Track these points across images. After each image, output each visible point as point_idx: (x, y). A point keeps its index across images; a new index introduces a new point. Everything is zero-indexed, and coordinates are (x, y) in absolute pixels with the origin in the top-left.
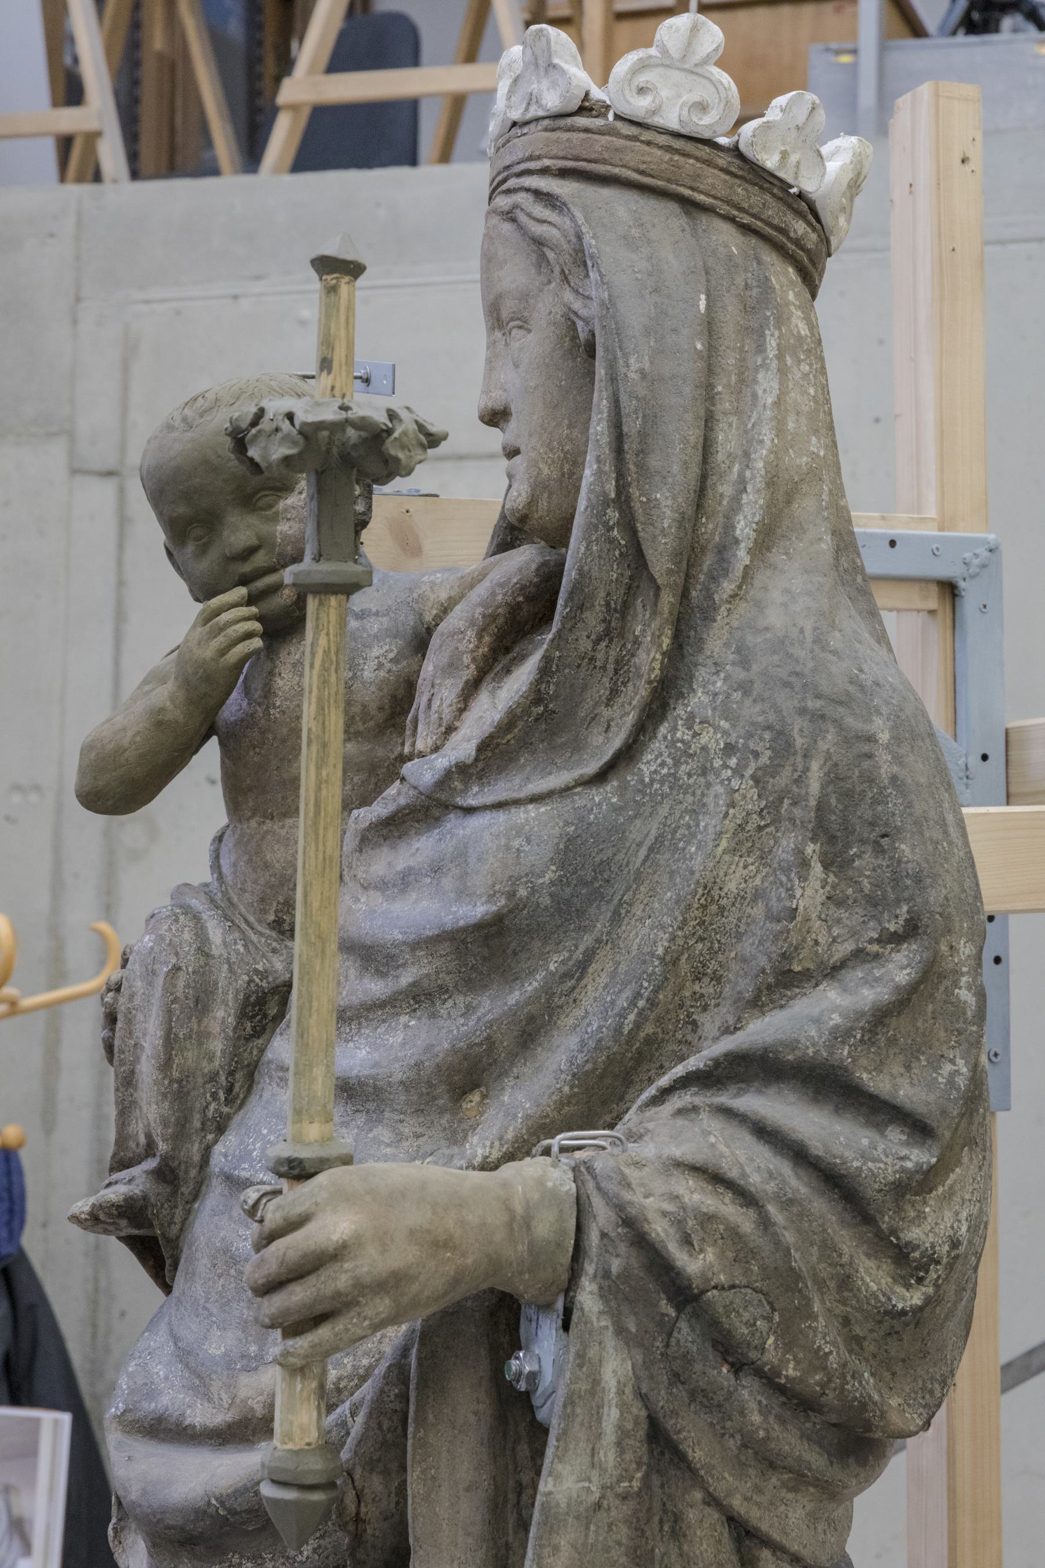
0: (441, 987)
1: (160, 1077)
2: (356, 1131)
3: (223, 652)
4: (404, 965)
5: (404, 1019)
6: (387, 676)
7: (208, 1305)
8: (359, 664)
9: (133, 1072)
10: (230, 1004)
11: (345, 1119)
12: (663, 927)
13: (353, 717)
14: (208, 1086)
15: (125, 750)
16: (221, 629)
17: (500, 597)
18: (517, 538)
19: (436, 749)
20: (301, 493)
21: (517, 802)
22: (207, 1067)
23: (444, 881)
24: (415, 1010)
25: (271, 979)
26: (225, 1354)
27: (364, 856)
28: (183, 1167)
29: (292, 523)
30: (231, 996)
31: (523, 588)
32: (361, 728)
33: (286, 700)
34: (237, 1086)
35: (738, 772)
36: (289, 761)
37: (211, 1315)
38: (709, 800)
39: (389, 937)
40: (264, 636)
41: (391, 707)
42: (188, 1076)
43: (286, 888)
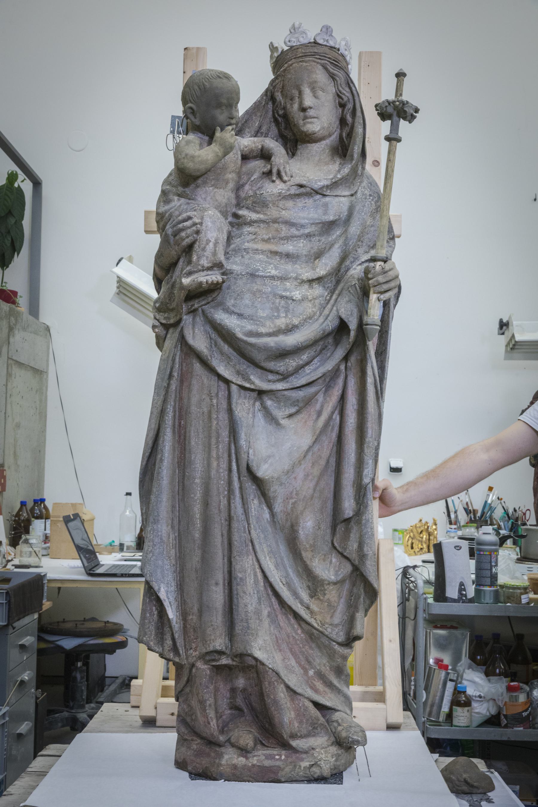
5: (302, 241)
9: (205, 247)
12: (358, 229)
19: (289, 180)
21: (340, 196)
26: (267, 316)
27: (281, 202)
35: (372, 200)
38: (366, 205)
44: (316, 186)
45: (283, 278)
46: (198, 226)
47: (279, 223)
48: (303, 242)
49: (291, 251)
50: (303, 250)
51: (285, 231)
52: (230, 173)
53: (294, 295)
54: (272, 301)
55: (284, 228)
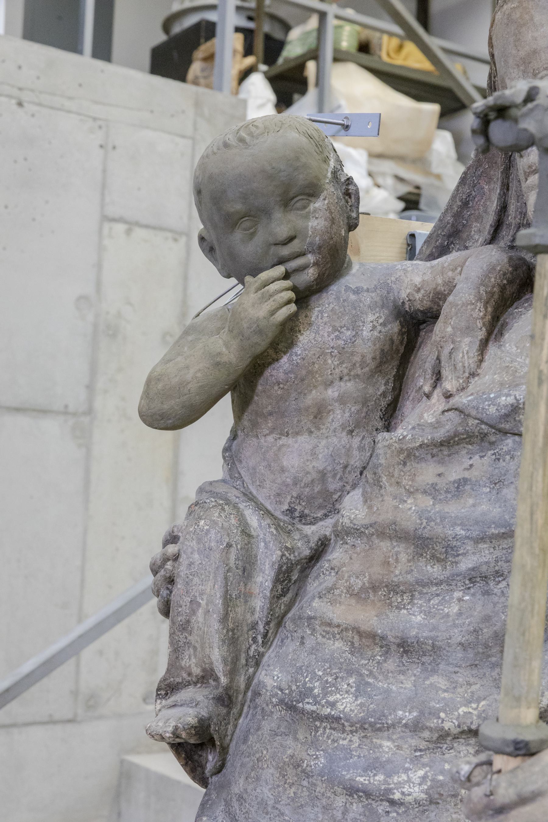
0: (497, 572)
1: (221, 627)
2: (413, 678)
3: (273, 313)
4: (464, 554)
5: (457, 594)
6: (379, 335)
7: (277, 806)
8: (359, 326)
9: (188, 622)
10: (267, 572)
11: (402, 668)
13: (355, 364)
14: (250, 633)
15: (189, 383)
16: (271, 296)
17: (493, 280)
18: (452, 243)
20: (325, 199)
22: (250, 619)
23: (505, 491)
24: (469, 588)
25: (296, 554)
27: (408, 468)
28: (235, 694)
29: (319, 220)
30: (267, 566)
31: (504, 274)
32: (359, 372)
33: (305, 350)
34: (270, 631)
36: (305, 394)
37: (283, 814)
39: (450, 532)
40: (296, 302)
41: (380, 358)
42: (238, 626)
43: (298, 486)
44: (492, 410)
45: (371, 726)
46: (169, 565)
47: (391, 538)
48: (460, 600)
49: (413, 633)
50: (455, 626)
51: (403, 564)
52: (329, 384)
53: (399, 785)
54: (324, 801)
55: (403, 557)
